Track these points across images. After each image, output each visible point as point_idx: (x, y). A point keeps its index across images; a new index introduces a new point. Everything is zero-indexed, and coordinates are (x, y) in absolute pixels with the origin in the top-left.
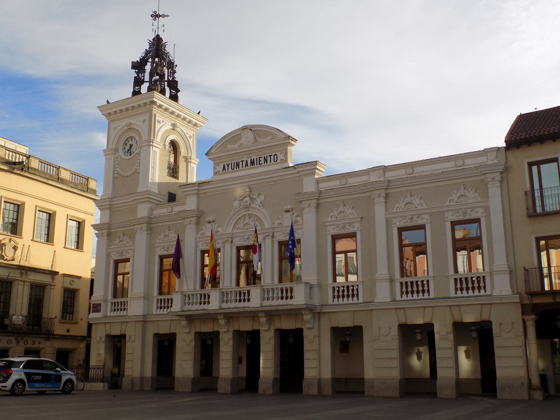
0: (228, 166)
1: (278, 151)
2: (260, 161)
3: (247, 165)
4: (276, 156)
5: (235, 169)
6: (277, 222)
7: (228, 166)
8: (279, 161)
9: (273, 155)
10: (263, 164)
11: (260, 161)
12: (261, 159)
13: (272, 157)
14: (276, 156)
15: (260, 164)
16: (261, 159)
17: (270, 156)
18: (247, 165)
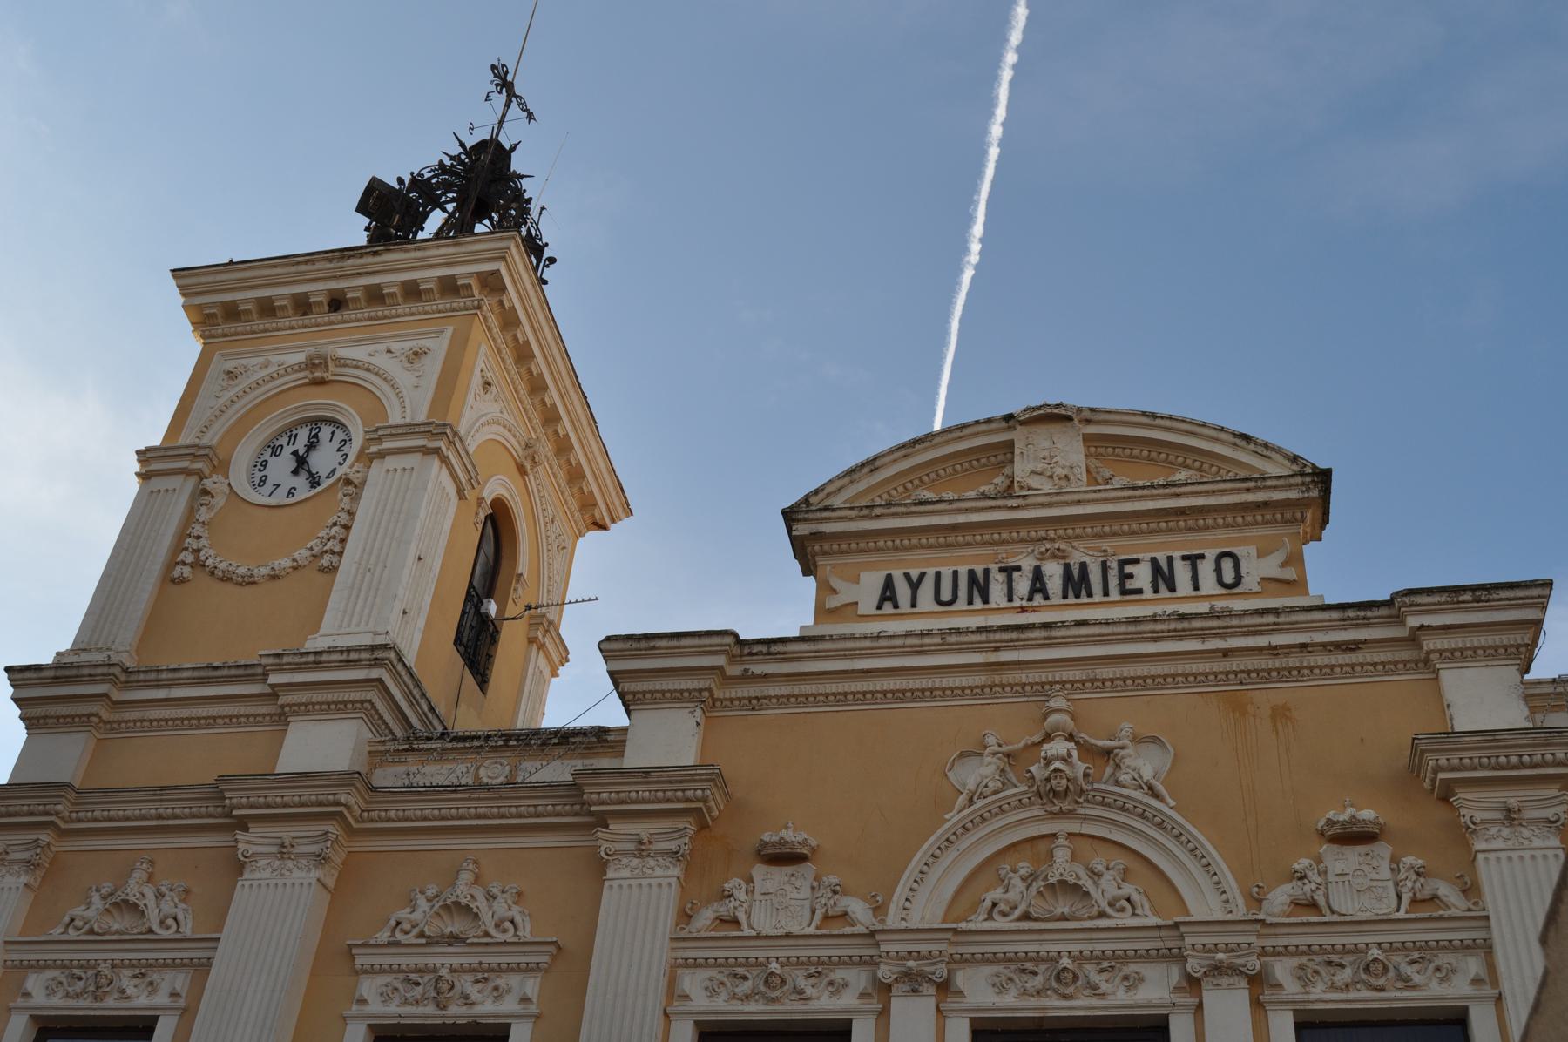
0: (915, 586)
1: (1244, 541)
2: (1124, 577)
3: (1038, 584)
4: (1227, 565)
5: (962, 604)
6: (1279, 898)
7: (915, 586)
8: (1250, 582)
9: (1211, 554)
10: (1148, 593)
11: (1124, 577)
12: (1128, 569)
13: (1206, 569)
14: (1227, 565)
15: (1124, 592)
16: (1128, 569)
17: (1193, 560)
18: (1038, 584)
